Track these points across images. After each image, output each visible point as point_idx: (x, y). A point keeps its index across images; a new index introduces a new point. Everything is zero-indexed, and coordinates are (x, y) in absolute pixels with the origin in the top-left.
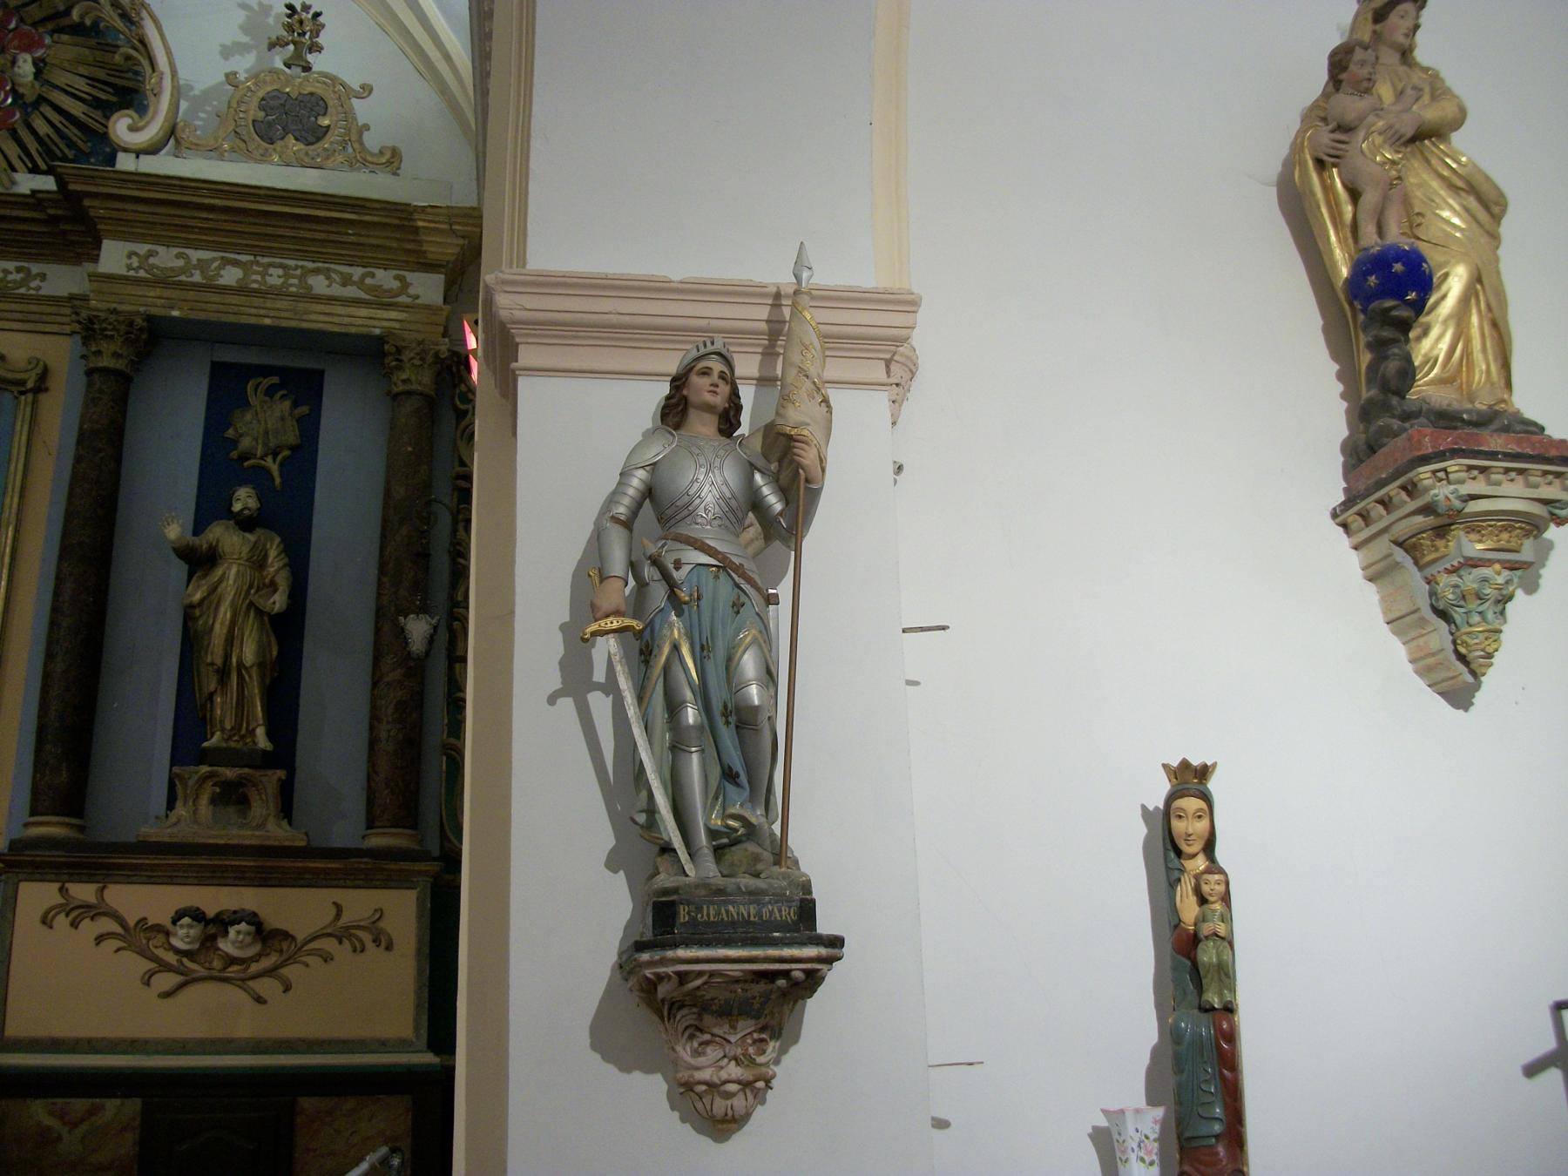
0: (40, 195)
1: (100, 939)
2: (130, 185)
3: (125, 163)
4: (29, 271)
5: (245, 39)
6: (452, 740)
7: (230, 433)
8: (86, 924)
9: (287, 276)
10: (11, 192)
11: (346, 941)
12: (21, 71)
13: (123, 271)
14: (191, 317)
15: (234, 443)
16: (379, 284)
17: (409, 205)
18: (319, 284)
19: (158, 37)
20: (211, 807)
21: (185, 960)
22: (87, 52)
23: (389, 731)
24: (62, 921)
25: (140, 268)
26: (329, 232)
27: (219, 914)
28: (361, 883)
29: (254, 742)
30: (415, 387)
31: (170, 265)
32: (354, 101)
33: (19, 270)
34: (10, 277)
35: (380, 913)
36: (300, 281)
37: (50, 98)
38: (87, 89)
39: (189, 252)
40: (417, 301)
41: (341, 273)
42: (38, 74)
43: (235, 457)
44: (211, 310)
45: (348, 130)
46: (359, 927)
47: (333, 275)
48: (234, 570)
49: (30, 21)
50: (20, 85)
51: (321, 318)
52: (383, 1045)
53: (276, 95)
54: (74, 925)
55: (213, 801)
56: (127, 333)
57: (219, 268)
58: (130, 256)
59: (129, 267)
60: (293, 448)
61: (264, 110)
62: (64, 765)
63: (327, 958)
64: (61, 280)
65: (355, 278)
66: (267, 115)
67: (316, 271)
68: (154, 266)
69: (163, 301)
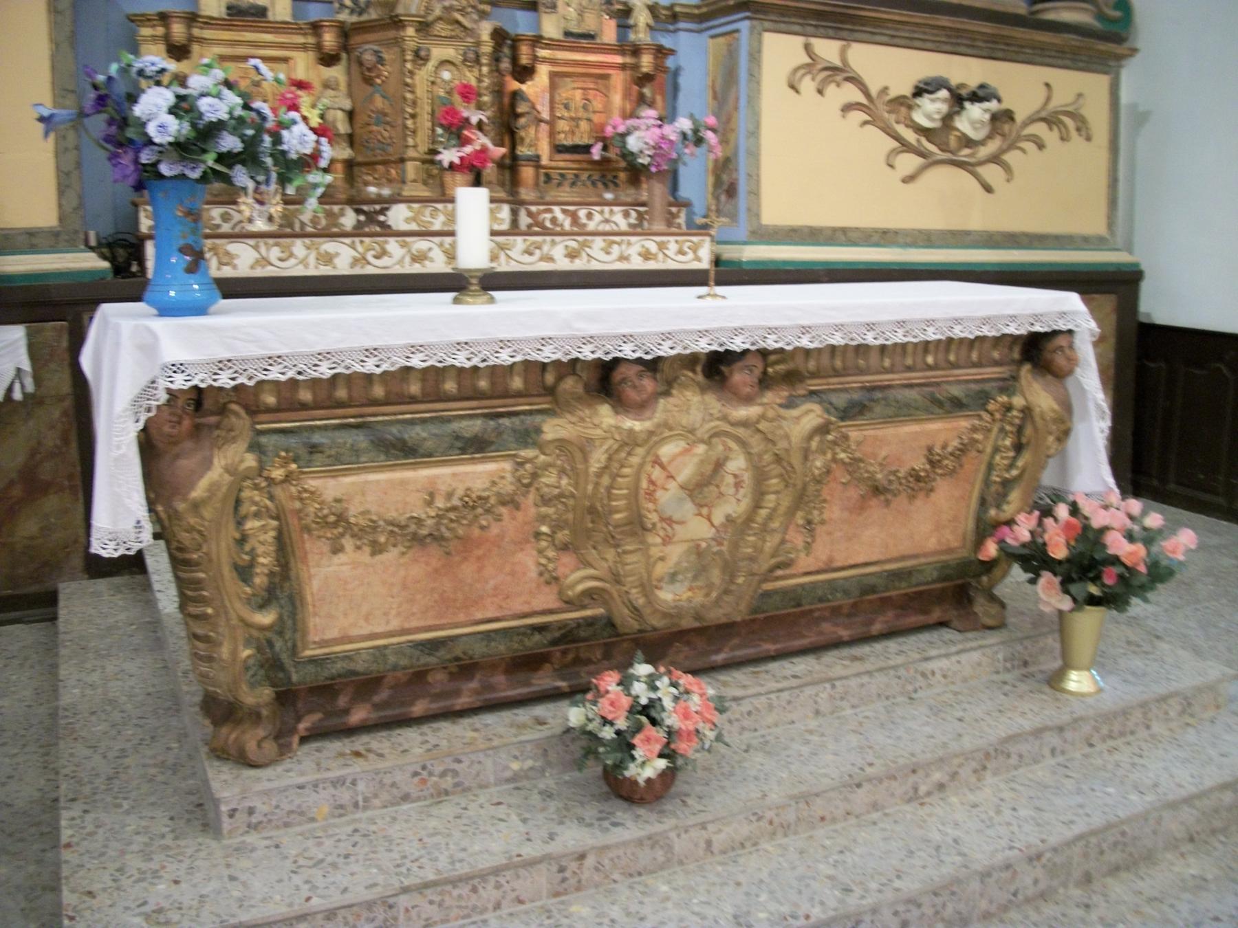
1: (847, 108)
8: (831, 89)
11: (1055, 128)
21: (924, 141)
24: (808, 85)
27: (962, 86)
28: (1068, 63)
52: (1085, 242)
63: (1041, 146)
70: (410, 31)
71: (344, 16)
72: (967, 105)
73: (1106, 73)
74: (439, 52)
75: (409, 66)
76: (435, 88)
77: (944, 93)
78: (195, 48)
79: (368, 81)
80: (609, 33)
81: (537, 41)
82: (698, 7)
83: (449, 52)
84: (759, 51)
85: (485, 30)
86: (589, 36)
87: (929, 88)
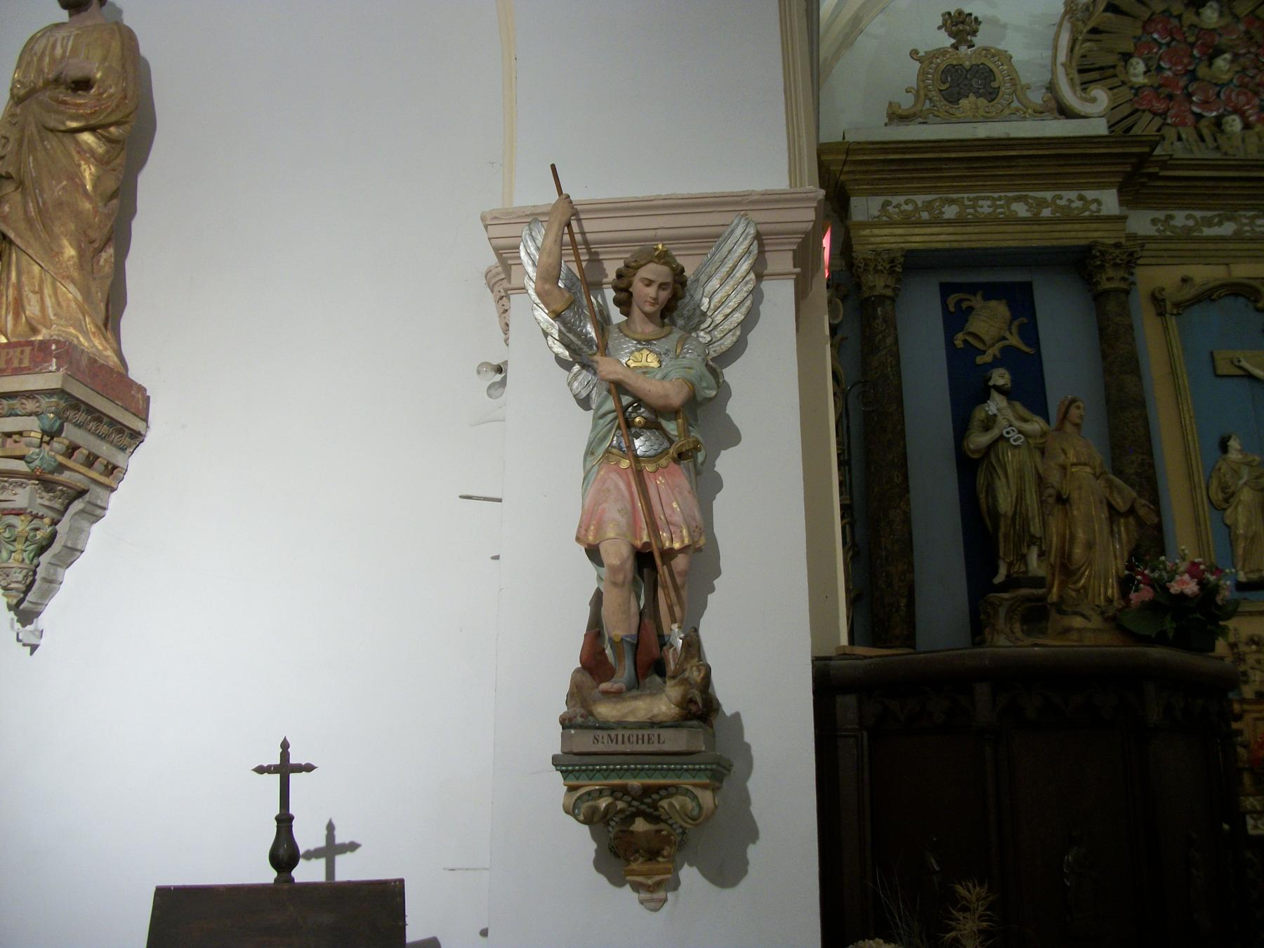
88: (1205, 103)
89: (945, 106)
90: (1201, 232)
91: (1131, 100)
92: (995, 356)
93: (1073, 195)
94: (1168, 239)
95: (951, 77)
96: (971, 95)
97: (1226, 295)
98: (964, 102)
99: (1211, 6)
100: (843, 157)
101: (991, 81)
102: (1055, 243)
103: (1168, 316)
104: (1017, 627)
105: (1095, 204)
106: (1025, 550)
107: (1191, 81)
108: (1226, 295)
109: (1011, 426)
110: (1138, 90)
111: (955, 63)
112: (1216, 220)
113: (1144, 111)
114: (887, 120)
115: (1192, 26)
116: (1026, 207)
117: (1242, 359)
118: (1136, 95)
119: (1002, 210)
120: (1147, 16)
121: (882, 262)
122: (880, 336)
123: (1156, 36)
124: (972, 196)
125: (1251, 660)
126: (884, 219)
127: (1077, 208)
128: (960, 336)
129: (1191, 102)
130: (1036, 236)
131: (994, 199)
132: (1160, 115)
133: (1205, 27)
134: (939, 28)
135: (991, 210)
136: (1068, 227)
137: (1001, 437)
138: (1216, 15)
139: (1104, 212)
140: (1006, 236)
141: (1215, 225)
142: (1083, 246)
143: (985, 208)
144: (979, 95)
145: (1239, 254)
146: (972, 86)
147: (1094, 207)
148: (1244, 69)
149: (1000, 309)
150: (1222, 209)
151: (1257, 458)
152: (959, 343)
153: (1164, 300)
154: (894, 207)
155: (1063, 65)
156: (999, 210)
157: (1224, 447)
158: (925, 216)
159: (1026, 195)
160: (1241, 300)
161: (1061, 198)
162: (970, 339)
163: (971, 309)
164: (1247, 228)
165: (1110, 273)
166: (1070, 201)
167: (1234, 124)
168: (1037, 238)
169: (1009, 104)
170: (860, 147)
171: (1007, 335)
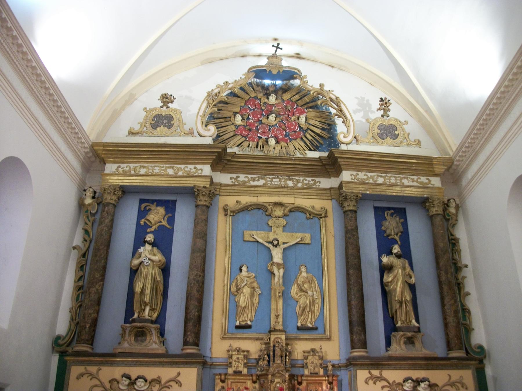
0: (321, 158)
1: (383, 387)
2: (353, 154)
3: (343, 147)
4: (315, 180)
5: (359, 108)
6: (464, 322)
7: (383, 228)
8: (378, 383)
9: (396, 180)
10: (305, 157)
11: (453, 387)
12: (302, 120)
13: (350, 180)
14: (373, 193)
15: (385, 232)
16: (422, 181)
17: (432, 157)
18: (406, 182)
19: (346, 110)
20: (404, 345)
22: (318, 114)
23: (453, 319)
24: (371, 382)
25: (355, 179)
26: (408, 166)
27: (417, 379)
28: (454, 368)
29: (411, 324)
30: (439, 212)
31: (363, 178)
32: (404, 125)
33: (313, 180)
34: (310, 183)
35: (461, 377)
36: (400, 181)
37: (310, 128)
38: (320, 125)
39: (368, 174)
40: (435, 186)
41: (411, 178)
42: (305, 122)
43: (386, 236)
44: (379, 191)
45: (404, 134)
46: (457, 382)
47: (409, 179)
48: (400, 271)
49: (300, 105)
50: (301, 124)
51: (409, 192)
53: (382, 125)
54: (375, 383)
55: (405, 343)
56: (356, 199)
57: (377, 178)
58: (351, 175)
59: (352, 179)
60: (402, 232)
61: (379, 130)
62: (362, 333)
64: (326, 183)
65: (415, 180)
66: (381, 131)
67: (404, 178)
68: (359, 178)
69: (364, 189)
70: (270, 376)
71: (258, 373)
72: (420, 383)
73: (470, 369)
74: (276, 380)
75: (269, 384)
76: (275, 388)
77: (410, 381)
78: (226, 381)
79: (262, 387)
80: (321, 372)
81: (302, 376)
82: (345, 364)
83: (279, 380)
84: (356, 375)
85: (287, 375)
86: (317, 374)
87: (406, 380)
88: (263, 133)
89: (151, 129)
90: (250, 183)
91: (235, 130)
92: (155, 229)
93: (192, 167)
94: (235, 185)
95: (157, 119)
96: (162, 126)
97: (254, 209)
98: (158, 129)
99: (272, 96)
100: (102, 148)
101: (171, 121)
102: (181, 185)
103: (228, 216)
104: (133, 338)
105: (201, 171)
106: (143, 307)
107: (260, 124)
108: (254, 209)
109: (146, 257)
110: (238, 127)
111: (159, 113)
112: (257, 179)
113: (239, 135)
114: (128, 134)
115: (265, 103)
116: (173, 171)
117: (254, 235)
118: (237, 129)
119: (163, 171)
120: (247, 98)
121: (110, 190)
122: (104, 218)
123: (249, 106)
124: (152, 165)
125: (234, 358)
126: (117, 173)
127: (193, 172)
128: (143, 220)
129: (258, 132)
130: (174, 182)
131: (161, 167)
132: (245, 137)
133: (270, 103)
134: (159, 100)
135: (159, 171)
136: (187, 179)
137: (142, 262)
138: (274, 99)
139: (204, 174)
140: (163, 182)
141: (256, 181)
142: (191, 187)
143: (157, 170)
144: (165, 126)
145: (263, 192)
146: (163, 122)
147: (200, 172)
148: (282, 120)
149: (161, 210)
150: (260, 175)
151: (254, 275)
152: (142, 223)
153: (227, 210)
154: (122, 168)
155: (200, 116)
156: (162, 171)
157: (241, 270)
158: (133, 172)
159: (174, 166)
160: (261, 211)
161: (187, 168)
162: (146, 221)
163: (150, 209)
164: (387, 180)
165: (201, 198)
166: (191, 169)
167: (272, 141)
168: (174, 183)
169: (176, 130)
170: (108, 144)
171: (162, 220)
